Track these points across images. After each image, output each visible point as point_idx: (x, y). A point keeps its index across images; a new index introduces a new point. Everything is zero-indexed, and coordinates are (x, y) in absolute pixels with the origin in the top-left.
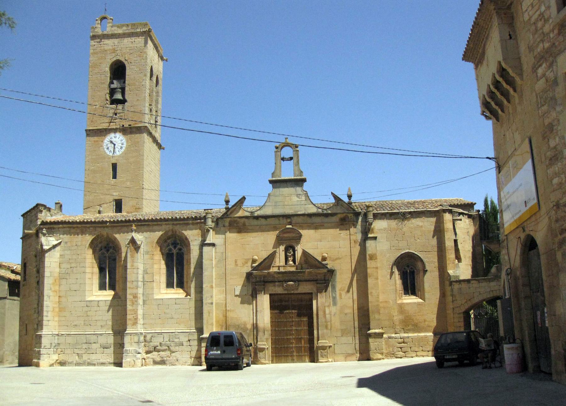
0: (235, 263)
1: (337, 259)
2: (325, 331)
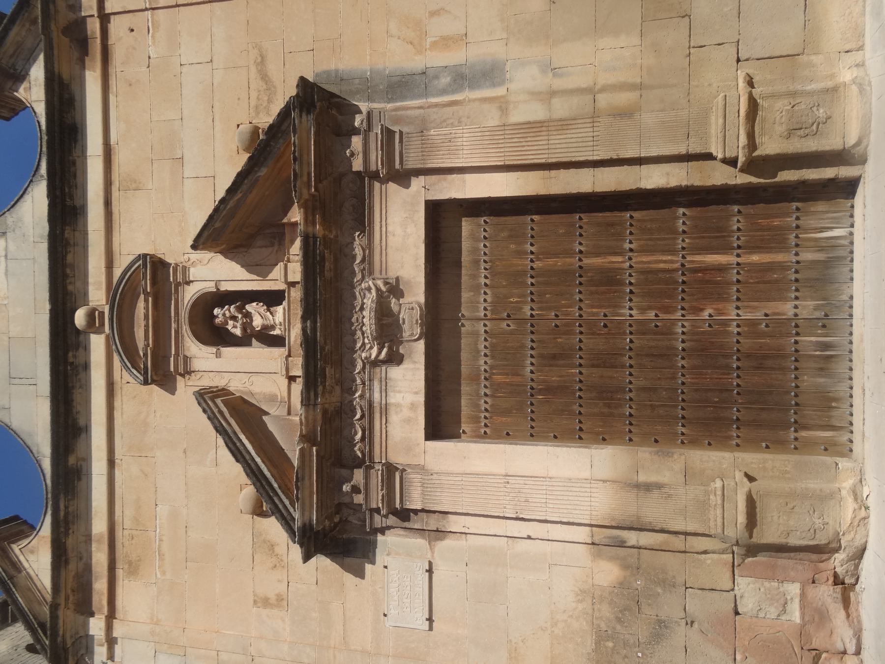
0: (272, 606)
1: (264, 77)
2: (648, 119)
